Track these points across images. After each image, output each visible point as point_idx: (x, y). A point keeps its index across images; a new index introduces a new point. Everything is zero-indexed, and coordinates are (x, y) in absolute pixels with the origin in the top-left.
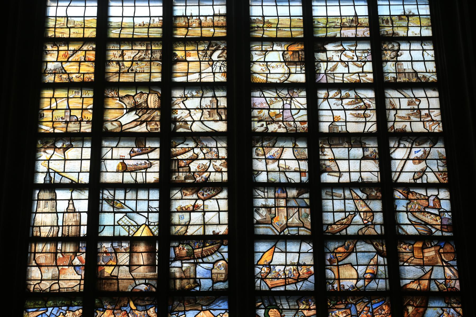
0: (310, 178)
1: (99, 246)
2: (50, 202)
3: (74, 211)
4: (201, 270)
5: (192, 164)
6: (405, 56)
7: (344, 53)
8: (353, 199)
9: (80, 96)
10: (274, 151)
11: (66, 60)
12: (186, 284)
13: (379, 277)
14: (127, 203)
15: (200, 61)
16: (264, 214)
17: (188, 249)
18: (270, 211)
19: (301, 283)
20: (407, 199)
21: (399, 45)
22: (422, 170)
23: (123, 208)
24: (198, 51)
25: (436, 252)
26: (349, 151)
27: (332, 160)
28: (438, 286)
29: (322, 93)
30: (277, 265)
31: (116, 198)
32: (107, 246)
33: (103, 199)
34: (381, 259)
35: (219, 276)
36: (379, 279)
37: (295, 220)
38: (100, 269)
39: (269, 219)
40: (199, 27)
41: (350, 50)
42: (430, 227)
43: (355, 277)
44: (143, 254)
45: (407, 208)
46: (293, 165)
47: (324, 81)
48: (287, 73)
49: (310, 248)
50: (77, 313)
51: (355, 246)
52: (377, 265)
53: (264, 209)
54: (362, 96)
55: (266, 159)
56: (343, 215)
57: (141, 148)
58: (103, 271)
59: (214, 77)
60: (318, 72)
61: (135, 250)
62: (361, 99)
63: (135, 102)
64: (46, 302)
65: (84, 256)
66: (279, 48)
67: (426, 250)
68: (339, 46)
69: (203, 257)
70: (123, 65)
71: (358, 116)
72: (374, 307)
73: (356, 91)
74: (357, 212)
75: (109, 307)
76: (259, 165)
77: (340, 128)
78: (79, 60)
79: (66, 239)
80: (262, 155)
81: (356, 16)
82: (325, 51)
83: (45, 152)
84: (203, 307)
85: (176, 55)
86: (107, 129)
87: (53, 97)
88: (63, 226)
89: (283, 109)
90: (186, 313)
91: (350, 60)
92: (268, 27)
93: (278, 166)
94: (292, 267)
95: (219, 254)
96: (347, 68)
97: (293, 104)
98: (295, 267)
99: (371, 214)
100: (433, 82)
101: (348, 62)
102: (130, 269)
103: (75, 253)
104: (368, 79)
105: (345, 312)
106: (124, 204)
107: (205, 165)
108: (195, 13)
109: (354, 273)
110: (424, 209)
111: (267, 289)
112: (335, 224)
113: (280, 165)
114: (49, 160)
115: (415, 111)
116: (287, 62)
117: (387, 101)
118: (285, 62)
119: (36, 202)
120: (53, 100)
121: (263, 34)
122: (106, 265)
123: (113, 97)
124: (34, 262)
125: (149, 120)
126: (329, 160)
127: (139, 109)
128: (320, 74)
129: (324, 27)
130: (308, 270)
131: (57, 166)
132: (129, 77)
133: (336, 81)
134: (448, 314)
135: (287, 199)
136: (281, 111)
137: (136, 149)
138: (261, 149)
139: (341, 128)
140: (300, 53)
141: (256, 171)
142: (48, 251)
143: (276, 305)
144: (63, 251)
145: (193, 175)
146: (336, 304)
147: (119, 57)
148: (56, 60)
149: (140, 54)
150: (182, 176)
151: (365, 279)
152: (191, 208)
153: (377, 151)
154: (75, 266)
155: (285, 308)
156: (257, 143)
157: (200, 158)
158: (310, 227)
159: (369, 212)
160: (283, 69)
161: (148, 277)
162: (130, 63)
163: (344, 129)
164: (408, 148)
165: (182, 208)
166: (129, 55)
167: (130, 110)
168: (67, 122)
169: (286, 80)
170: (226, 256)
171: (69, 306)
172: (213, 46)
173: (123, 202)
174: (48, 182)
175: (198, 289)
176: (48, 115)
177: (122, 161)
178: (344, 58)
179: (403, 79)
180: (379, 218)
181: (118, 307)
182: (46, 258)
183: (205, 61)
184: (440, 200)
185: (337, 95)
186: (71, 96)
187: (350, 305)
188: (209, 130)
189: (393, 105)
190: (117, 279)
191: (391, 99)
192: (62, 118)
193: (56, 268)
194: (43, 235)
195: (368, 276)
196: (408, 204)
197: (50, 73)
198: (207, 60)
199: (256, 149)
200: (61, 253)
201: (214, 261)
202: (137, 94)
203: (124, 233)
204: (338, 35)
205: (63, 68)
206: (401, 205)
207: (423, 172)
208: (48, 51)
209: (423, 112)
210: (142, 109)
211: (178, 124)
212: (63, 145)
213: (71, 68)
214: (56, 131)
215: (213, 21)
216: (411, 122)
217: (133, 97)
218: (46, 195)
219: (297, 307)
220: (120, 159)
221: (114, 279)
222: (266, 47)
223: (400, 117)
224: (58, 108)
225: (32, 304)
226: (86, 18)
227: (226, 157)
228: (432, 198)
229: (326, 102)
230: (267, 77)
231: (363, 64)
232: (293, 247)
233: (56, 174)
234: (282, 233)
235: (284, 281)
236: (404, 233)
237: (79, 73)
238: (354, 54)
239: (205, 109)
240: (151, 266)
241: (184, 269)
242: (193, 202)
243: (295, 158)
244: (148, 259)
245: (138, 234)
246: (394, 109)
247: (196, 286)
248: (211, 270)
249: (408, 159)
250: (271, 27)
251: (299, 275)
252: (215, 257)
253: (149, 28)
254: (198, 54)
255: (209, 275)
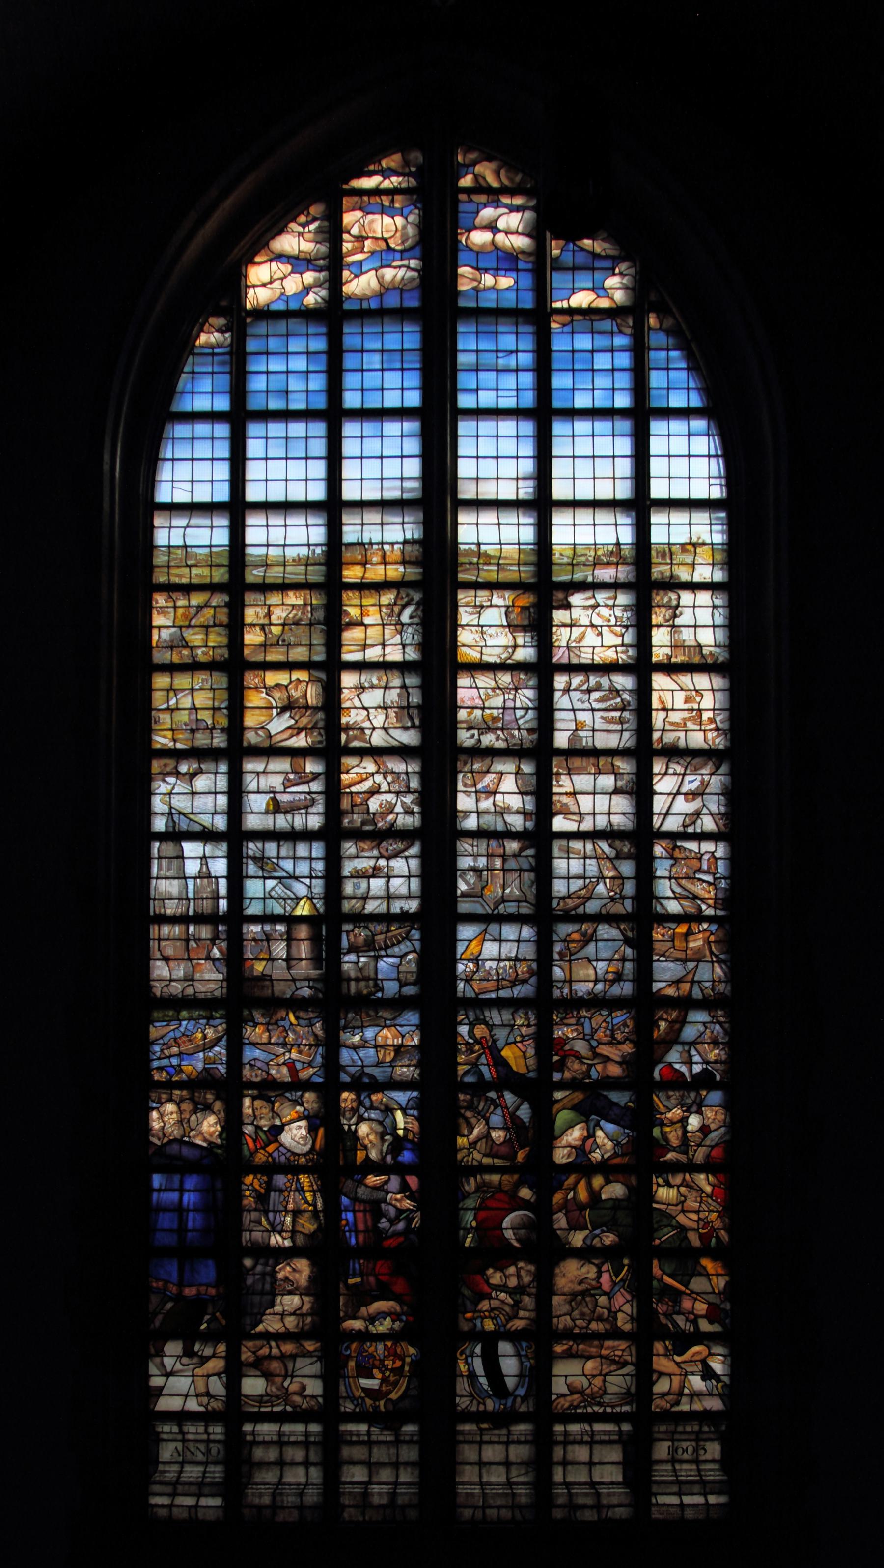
0: (537, 825)
1: (245, 930)
2: (175, 862)
3: (209, 876)
4: (385, 965)
5: (372, 799)
6: (685, 618)
7: (596, 611)
8: (596, 858)
9: (209, 687)
10: (489, 779)
11: (187, 623)
12: (364, 988)
13: (625, 978)
14: (282, 863)
15: (383, 625)
16: (472, 881)
17: (367, 936)
18: (480, 877)
19: (519, 987)
20: (672, 857)
21: (679, 597)
22: (696, 811)
23: (275, 871)
24: (380, 606)
25: (704, 941)
26: (595, 780)
27: (570, 794)
28: (702, 991)
29: (560, 681)
30: (487, 960)
31: (266, 855)
32: (256, 928)
33: (248, 857)
34: (629, 951)
35: (408, 976)
36: (625, 981)
37: (512, 890)
38: (248, 964)
39: (478, 889)
40: (381, 564)
41: (606, 606)
42: (699, 903)
43: (593, 978)
44: (305, 942)
45: (670, 872)
46: (515, 802)
47: (565, 660)
48: (511, 647)
49: (534, 934)
50: (220, 1028)
51: (595, 931)
52: (623, 960)
53: (472, 873)
54: (619, 687)
55: (476, 792)
56: (580, 882)
57: (298, 773)
58: (252, 968)
59: (404, 653)
60: (556, 644)
61: (294, 936)
62: (618, 691)
63: (289, 697)
64: (179, 1013)
65: (224, 945)
66: (500, 602)
67: (691, 938)
68: (590, 598)
69: (387, 947)
70: (271, 632)
71: (611, 721)
72: (615, 1022)
73: (612, 678)
74: (601, 878)
75: (262, 1020)
76: (464, 802)
77: (584, 740)
78: (206, 624)
79: (199, 919)
80: (471, 786)
81: (618, 544)
82: (568, 606)
83: (164, 781)
84: (388, 1022)
85: (348, 614)
86: (249, 743)
87: (171, 689)
88: (194, 899)
89: (504, 708)
90: (365, 1030)
91: (605, 624)
92: (485, 564)
93: (494, 805)
94: (507, 963)
95: (408, 943)
96: (600, 637)
97: (518, 700)
98: (512, 963)
99: (621, 881)
100: (723, 663)
101: (601, 626)
102: (288, 964)
103: (213, 941)
104: (628, 657)
105: (576, 1030)
106: (278, 865)
107: (390, 803)
108: (377, 538)
109: (591, 972)
110: (694, 873)
111: (473, 996)
112: (569, 896)
113: (497, 803)
114: (170, 794)
115: (695, 713)
116: (512, 627)
117: (655, 696)
118: (509, 626)
119: (156, 861)
120: (172, 694)
121: (477, 577)
122: (256, 959)
123: (256, 688)
124: (158, 953)
125: (310, 726)
126: (566, 794)
127: (294, 708)
128: (559, 647)
129: (569, 564)
130: (529, 967)
131: (181, 803)
132: (278, 653)
133: (583, 661)
134: (712, 1032)
135: (504, 857)
136: (501, 711)
137: (292, 776)
138: (469, 775)
139: (586, 739)
140: (532, 610)
141: (462, 812)
142: (177, 937)
143: (484, 1019)
144: (197, 937)
145: (373, 819)
146: (565, 1018)
147: (265, 617)
148: (171, 624)
149: (294, 612)
150: (357, 819)
151: (605, 981)
152: (371, 870)
153: (635, 780)
154: (214, 960)
155: (497, 1023)
156: (465, 764)
157: (382, 790)
158: (534, 902)
159: (618, 878)
160: (504, 639)
161: (313, 976)
162: (280, 628)
163: (590, 744)
164: (679, 774)
165: (357, 871)
166: (279, 615)
167: (283, 710)
168: (193, 731)
169: (509, 658)
170: (418, 945)
171: (209, 1018)
172: (402, 598)
173: (275, 861)
174: (171, 829)
175: (379, 995)
176: (165, 718)
177: (272, 795)
178: (597, 621)
179: (679, 659)
180: (629, 888)
181: (273, 1021)
182: (175, 948)
183: (391, 625)
184: (716, 859)
185: (584, 684)
186: (197, 687)
187: (582, 1020)
188: (395, 743)
189: (662, 702)
190: (271, 980)
191: (661, 693)
192: (186, 725)
193: (190, 965)
194: (169, 912)
195: (610, 976)
196: (672, 866)
197: (166, 647)
198: (393, 622)
199: (464, 776)
200: (195, 940)
201: (401, 954)
202: (291, 682)
203: (278, 910)
204: (590, 579)
205: (183, 637)
206: (662, 869)
207: (698, 814)
208: (161, 607)
209: (706, 715)
210: (299, 708)
211: (351, 733)
212: (189, 769)
213: (195, 638)
214: (179, 746)
215: (403, 552)
216: (686, 731)
217: (286, 687)
218: (169, 848)
219: (512, 1022)
220: (270, 792)
221: (267, 980)
222: (482, 596)
223: (672, 724)
224: (180, 706)
225: (160, 1015)
226: (214, 549)
227: (420, 790)
228: (706, 857)
229: (566, 697)
230: (482, 653)
231: (624, 630)
232: (509, 931)
233: (182, 817)
234: (496, 912)
235: (496, 983)
236: (663, 912)
237: (206, 646)
238: (611, 613)
239: (391, 708)
240: (316, 960)
241: (360, 965)
242: (372, 863)
243: (517, 791)
244: (313, 951)
245: (298, 912)
246: (664, 709)
247: (377, 992)
248: (398, 967)
249: (678, 793)
250: (490, 564)
251: (517, 975)
252: (404, 947)
253: (307, 565)
254: (380, 611)
255: (394, 975)
